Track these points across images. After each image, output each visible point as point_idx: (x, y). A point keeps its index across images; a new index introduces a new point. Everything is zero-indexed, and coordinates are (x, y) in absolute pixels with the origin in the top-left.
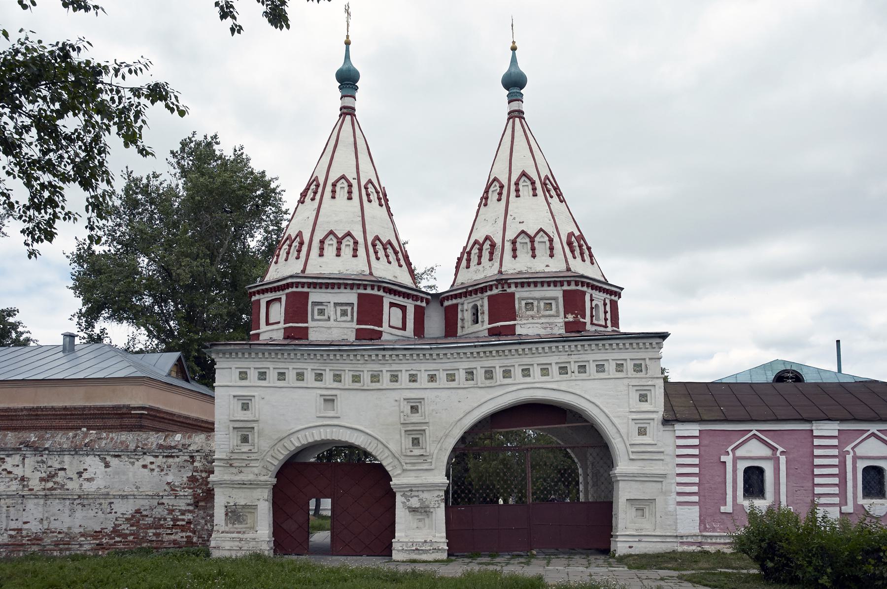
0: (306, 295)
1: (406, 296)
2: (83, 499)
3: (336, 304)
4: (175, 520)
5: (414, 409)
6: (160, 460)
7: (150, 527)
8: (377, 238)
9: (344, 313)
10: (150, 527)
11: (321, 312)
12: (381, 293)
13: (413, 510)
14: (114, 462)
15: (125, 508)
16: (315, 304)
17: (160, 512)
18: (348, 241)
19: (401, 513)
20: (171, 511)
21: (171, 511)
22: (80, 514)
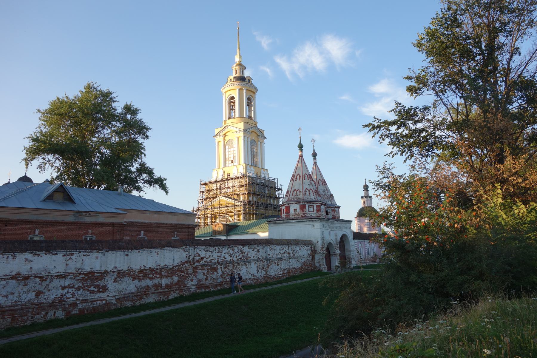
7: (307, 265)
10: (307, 265)
15: (303, 260)
17: (307, 261)
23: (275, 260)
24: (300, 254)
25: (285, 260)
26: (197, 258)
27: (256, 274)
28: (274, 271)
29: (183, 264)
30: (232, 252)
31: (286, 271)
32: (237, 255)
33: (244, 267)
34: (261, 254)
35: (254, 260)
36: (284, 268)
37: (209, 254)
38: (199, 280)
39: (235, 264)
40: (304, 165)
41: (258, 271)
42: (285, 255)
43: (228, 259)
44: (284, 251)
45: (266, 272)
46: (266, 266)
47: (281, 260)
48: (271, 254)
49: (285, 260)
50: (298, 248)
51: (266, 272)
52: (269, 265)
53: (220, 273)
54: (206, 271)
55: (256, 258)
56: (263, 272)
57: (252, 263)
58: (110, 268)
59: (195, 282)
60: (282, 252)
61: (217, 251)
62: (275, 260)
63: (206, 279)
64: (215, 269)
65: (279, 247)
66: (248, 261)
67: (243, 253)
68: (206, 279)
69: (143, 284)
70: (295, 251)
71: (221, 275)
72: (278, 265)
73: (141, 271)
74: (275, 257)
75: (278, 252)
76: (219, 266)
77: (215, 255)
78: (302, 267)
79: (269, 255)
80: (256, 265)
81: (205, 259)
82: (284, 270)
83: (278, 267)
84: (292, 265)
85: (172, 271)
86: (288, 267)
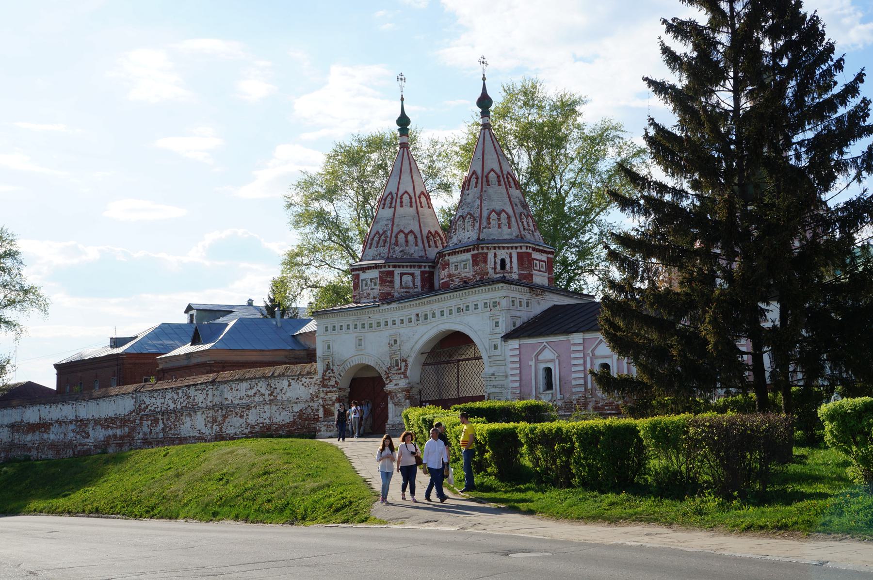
0: (358, 275)
1: (414, 266)
2: (283, 406)
3: (371, 280)
4: (314, 415)
5: (395, 341)
6: (308, 381)
8: (401, 231)
9: (375, 284)
10: (306, 419)
11: (366, 285)
12: (391, 269)
13: (396, 404)
14: (293, 382)
15: (297, 408)
16: (363, 280)
17: (309, 411)
18: (383, 238)
19: (390, 406)
20: (313, 410)
21: (313, 410)
23: (235, 407)
24: (288, 395)
25: (255, 407)
26: (143, 406)
27: (203, 431)
29: (131, 413)
30: (176, 397)
31: (257, 429)
32: (182, 400)
33: (188, 419)
34: (210, 398)
35: (200, 408)
36: (253, 423)
37: (153, 400)
38: (145, 434)
39: (177, 413)
40: (406, 166)
41: (206, 425)
42: (256, 399)
43: (172, 406)
44: (254, 390)
45: (221, 429)
46: (219, 419)
47: (248, 407)
48: (230, 398)
49: (255, 407)
50: (285, 383)
51: (221, 429)
52: (225, 417)
53: (161, 426)
54: (149, 423)
55: (204, 405)
56: (215, 427)
57: (199, 413)
58: (91, 417)
59: (141, 436)
60: (250, 393)
61: (160, 396)
63: (151, 433)
64: (156, 421)
65: (244, 385)
66: (192, 409)
67: (189, 397)
68: (151, 433)
69: (110, 432)
70: (278, 390)
71: (163, 429)
72: (241, 417)
73: (106, 420)
76: (160, 417)
78: (294, 422)
79: (226, 399)
80: (204, 416)
81: (149, 408)
82: (252, 427)
83: (242, 421)
84: (270, 418)
85: (123, 421)
86: (261, 421)
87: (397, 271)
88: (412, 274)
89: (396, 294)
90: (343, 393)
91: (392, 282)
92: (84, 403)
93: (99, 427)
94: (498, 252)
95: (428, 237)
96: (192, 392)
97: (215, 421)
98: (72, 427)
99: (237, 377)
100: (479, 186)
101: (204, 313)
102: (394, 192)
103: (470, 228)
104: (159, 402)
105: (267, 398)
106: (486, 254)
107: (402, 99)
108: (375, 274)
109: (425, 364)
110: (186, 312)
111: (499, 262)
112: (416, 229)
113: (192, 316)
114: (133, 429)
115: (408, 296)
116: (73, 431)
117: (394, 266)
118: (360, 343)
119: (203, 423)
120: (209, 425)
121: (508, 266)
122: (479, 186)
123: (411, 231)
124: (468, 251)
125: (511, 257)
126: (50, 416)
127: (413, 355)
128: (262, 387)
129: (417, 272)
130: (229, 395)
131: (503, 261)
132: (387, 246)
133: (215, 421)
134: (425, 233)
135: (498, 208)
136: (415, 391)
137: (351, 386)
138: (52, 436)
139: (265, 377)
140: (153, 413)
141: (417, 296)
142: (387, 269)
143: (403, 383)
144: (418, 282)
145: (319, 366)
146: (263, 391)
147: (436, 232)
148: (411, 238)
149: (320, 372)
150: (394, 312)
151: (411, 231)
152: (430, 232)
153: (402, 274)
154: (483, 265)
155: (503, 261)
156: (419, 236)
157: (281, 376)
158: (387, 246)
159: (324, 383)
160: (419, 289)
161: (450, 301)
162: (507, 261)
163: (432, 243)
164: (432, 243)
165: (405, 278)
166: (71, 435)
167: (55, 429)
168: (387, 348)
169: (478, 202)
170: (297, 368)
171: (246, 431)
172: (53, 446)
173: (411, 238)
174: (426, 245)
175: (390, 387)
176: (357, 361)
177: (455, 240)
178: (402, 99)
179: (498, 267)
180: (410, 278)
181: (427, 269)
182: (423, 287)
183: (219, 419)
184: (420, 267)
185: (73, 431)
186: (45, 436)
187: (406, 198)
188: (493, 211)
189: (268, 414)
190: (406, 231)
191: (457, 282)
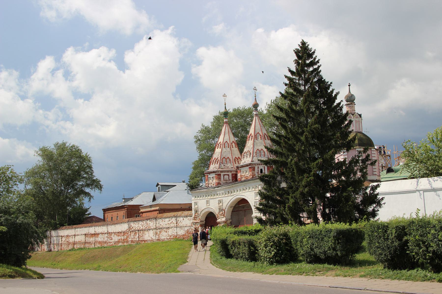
6: (190, 218)
12: (220, 173)
17: (190, 230)
22: (182, 231)
24: (183, 223)
28: (164, 236)
31: (172, 237)
33: (147, 233)
36: (171, 235)
38: (132, 239)
43: (141, 227)
44: (171, 221)
46: (158, 233)
47: (168, 228)
52: (160, 232)
53: (137, 235)
57: (151, 231)
59: (130, 240)
60: (169, 222)
62: (164, 228)
65: (167, 219)
69: (120, 238)
70: (179, 222)
73: (118, 233)
74: (164, 226)
75: (167, 223)
77: (137, 226)
80: (153, 232)
82: (170, 236)
83: (167, 234)
86: (173, 234)
87: (222, 174)
88: (228, 175)
89: (222, 183)
90: (202, 223)
91: (220, 178)
92: (110, 226)
93: (116, 236)
94: (259, 166)
95: (235, 160)
96: (148, 222)
97: (156, 233)
98: (106, 235)
99: (165, 216)
100: (253, 139)
101: (164, 187)
102: (222, 141)
103: (249, 157)
104: (137, 226)
105: (175, 224)
106: (255, 167)
107: (225, 104)
108: (213, 175)
109: (232, 211)
110: (157, 186)
111: (260, 170)
112: (230, 157)
113: (159, 187)
114: (128, 237)
115: (227, 183)
116: (107, 237)
117: (221, 172)
118: (208, 202)
119: (153, 234)
120: (155, 235)
121: (263, 172)
122: (253, 139)
123: (228, 158)
124: (248, 166)
125: (264, 168)
126: (99, 231)
127: (227, 207)
128: (174, 220)
129: (230, 174)
130: (161, 223)
131: (261, 170)
132: (218, 163)
133: (156, 233)
134: (234, 158)
135: (260, 148)
136: (229, 222)
137: (205, 220)
138: (100, 238)
139: (174, 216)
140: (135, 231)
141: (231, 183)
142: (218, 173)
143: (224, 219)
144: (231, 178)
145: (193, 212)
146: (174, 222)
147: (239, 157)
148: (228, 160)
149: (194, 214)
150: (221, 191)
151: (228, 158)
152: (236, 157)
153: (224, 175)
154: (253, 172)
155: (261, 170)
156: (231, 159)
157: (180, 216)
158: (218, 163)
159: (195, 218)
160: (231, 181)
161: (239, 186)
162: (263, 170)
163: (237, 162)
164: (237, 162)
165: (225, 176)
166: (106, 239)
167: (100, 236)
168: (217, 205)
169: (252, 146)
170: (186, 213)
171: (168, 238)
172: (100, 242)
173: (228, 160)
174: (234, 163)
175: (219, 220)
176: (206, 210)
177: (243, 161)
178: (225, 104)
179: (260, 172)
180: (227, 176)
181: (234, 173)
182: (232, 180)
183: (158, 233)
184: (231, 172)
185: (107, 237)
186: (97, 239)
187: (226, 144)
188: (258, 149)
189: (175, 231)
190: (226, 157)
191: (243, 179)
